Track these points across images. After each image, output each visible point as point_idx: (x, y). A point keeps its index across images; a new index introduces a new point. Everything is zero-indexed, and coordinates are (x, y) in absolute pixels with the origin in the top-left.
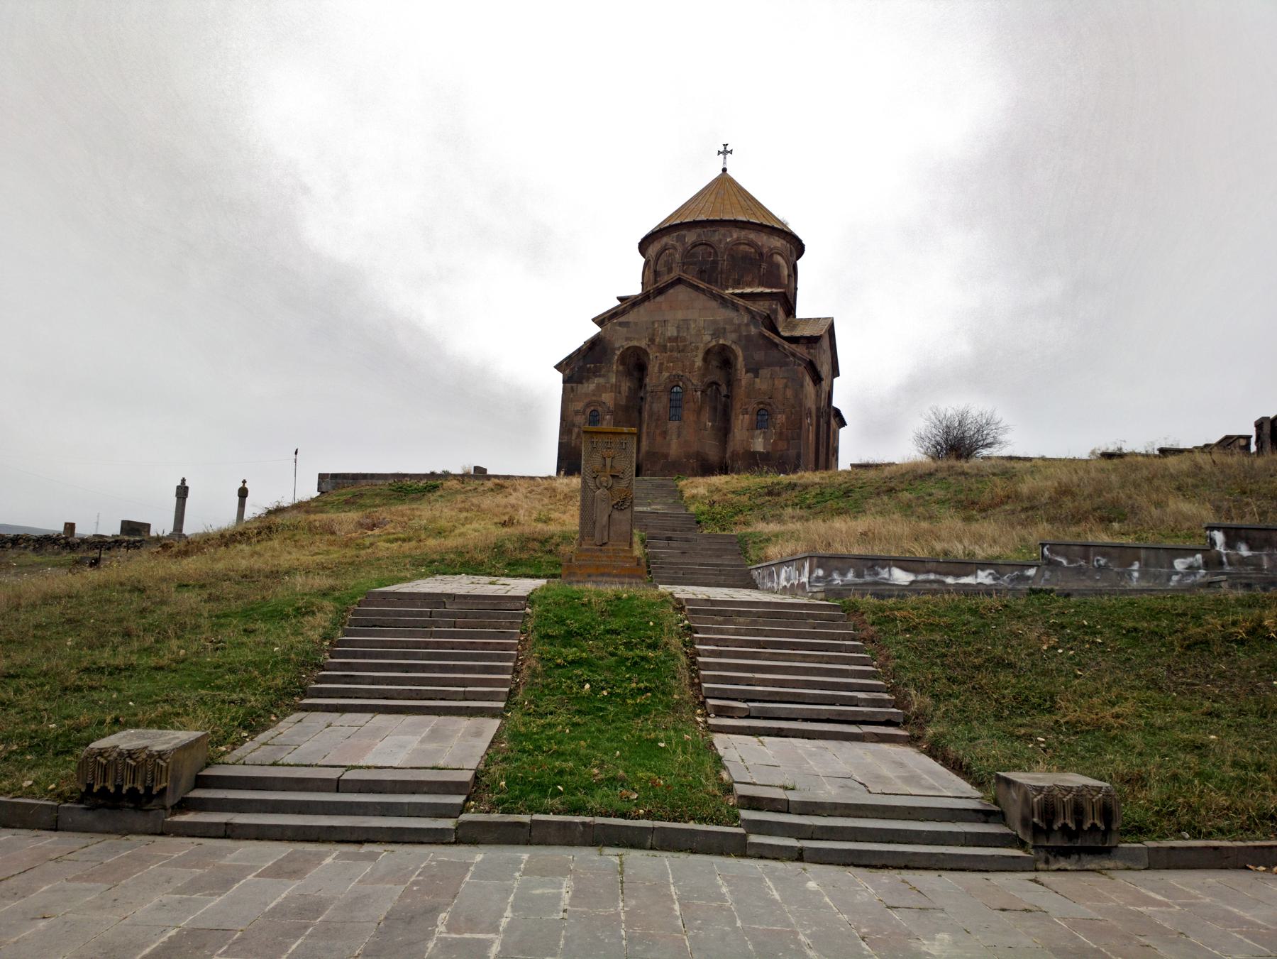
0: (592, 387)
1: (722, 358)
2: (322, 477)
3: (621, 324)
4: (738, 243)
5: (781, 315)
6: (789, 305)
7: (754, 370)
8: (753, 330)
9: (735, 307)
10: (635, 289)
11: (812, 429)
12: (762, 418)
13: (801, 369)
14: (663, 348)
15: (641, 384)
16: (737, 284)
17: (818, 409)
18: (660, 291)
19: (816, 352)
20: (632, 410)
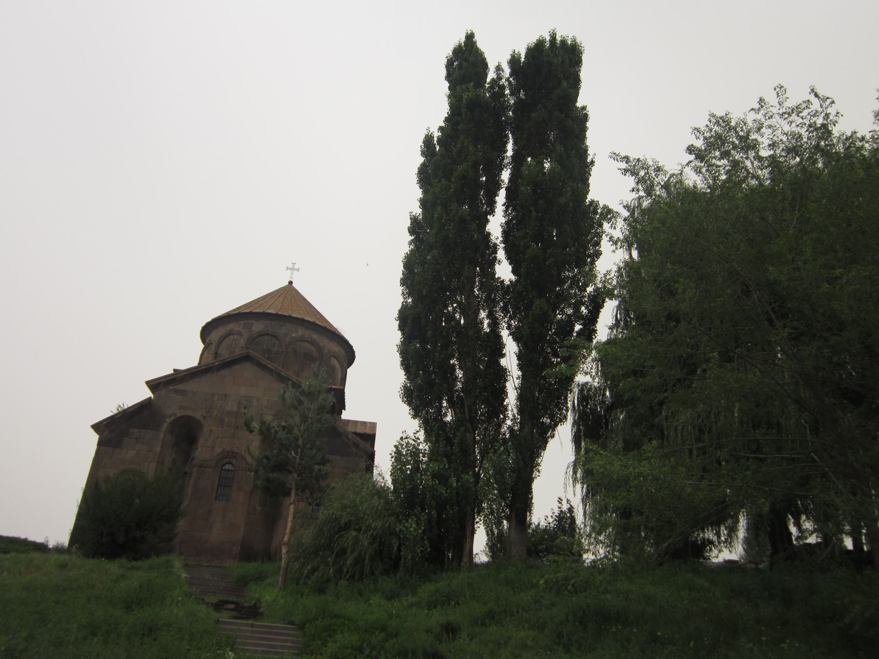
0: (131, 453)
4: (302, 339)
15: (187, 457)
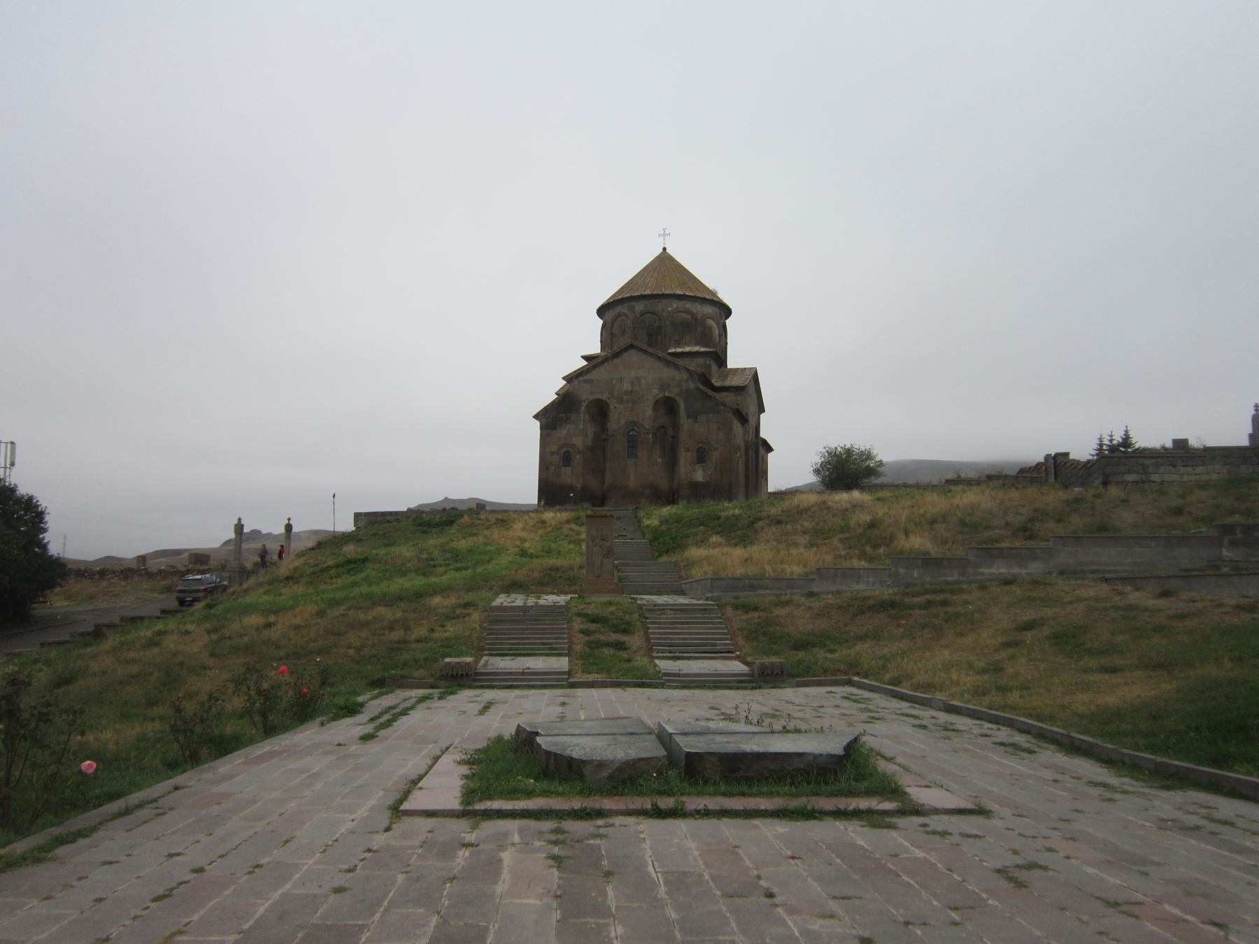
0: (564, 432)
1: (668, 406)
2: (357, 515)
3: (585, 381)
4: (677, 311)
5: (714, 367)
6: (720, 357)
7: (693, 415)
8: (692, 385)
9: (676, 367)
10: (595, 348)
11: (742, 461)
12: (701, 457)
13: (730, 415)
14: (621, 401)
16: (678, 344)
17: (747, 442)
18: (617, 355)
19: (743, 397)
20: (599, 448)
